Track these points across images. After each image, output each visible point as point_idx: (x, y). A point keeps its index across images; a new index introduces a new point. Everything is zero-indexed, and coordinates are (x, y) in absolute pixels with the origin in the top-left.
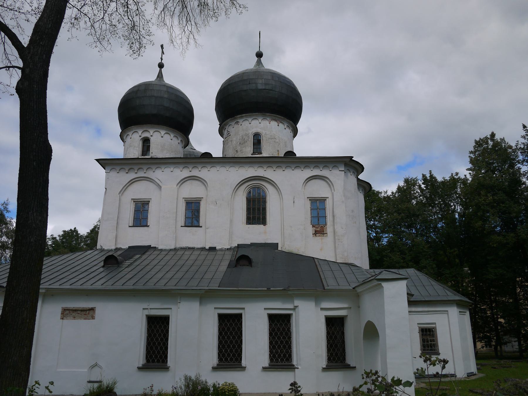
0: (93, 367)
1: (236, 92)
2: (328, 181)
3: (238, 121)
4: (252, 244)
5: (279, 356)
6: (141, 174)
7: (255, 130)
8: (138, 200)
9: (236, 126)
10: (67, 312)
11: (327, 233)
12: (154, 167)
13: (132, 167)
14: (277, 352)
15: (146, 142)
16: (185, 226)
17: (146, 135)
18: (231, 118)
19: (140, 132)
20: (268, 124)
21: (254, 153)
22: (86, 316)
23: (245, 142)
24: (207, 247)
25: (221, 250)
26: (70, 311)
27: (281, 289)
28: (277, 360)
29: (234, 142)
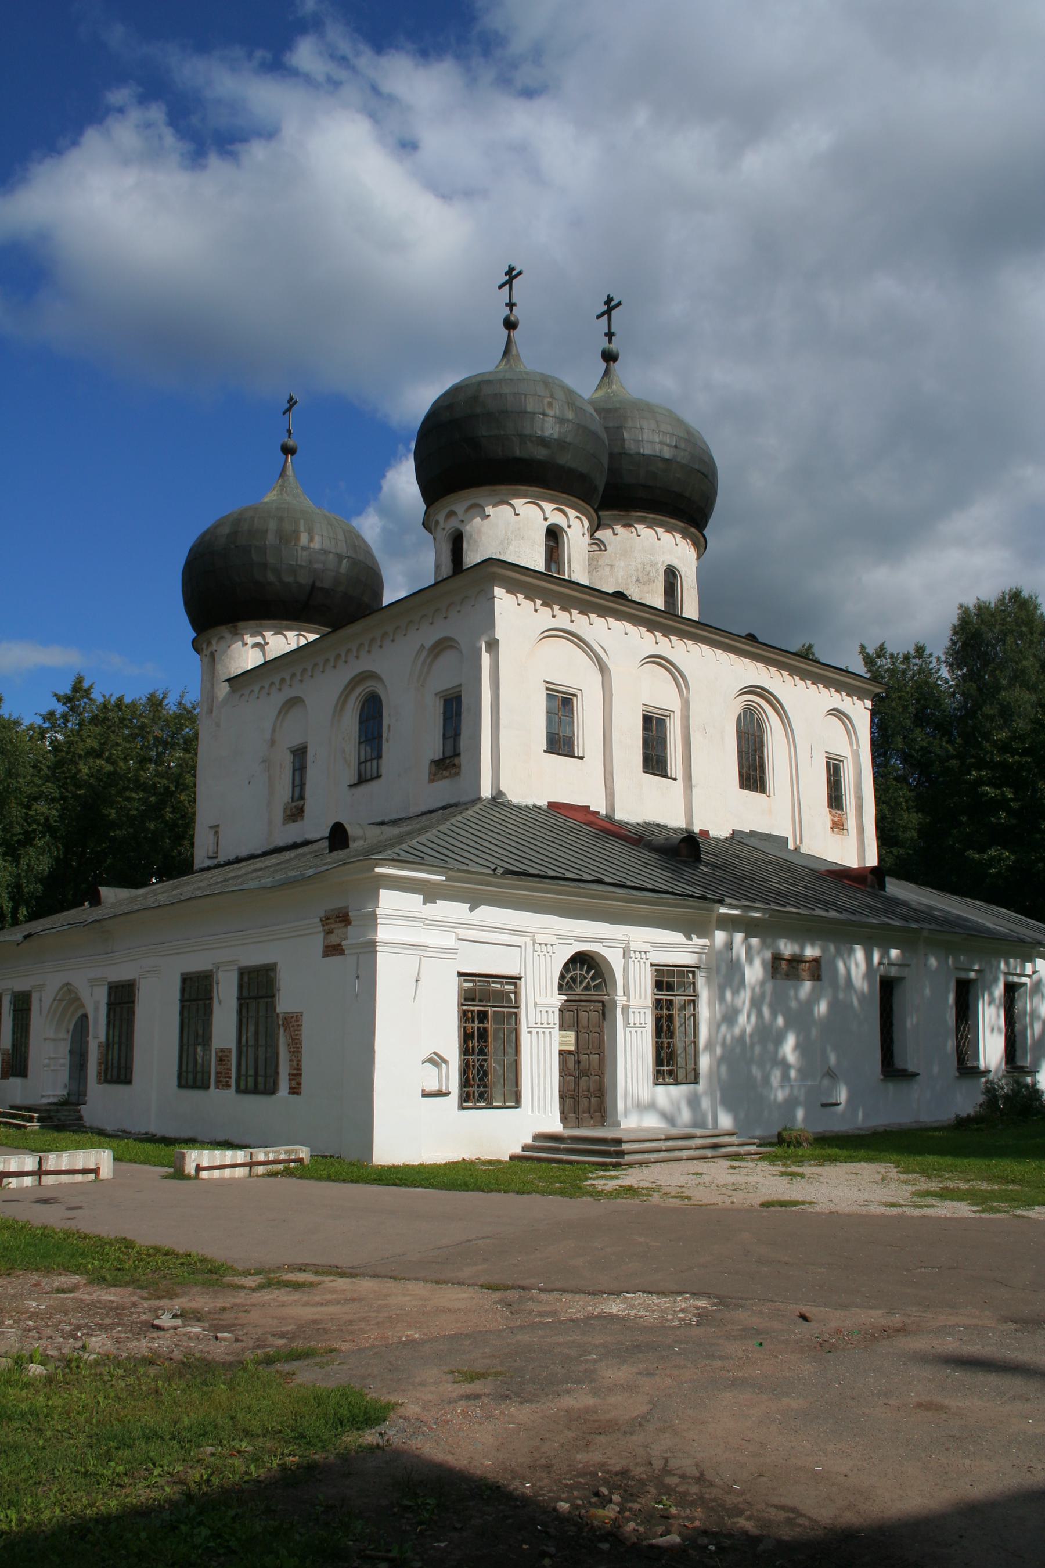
1: (643, 455)
8: (556, 687)
11: (847, 830)
15: (554, 534)
17: (557, 519)
18: (621, 511)
19: (548, 507)
23: (651, 581)
29: (621, 573)
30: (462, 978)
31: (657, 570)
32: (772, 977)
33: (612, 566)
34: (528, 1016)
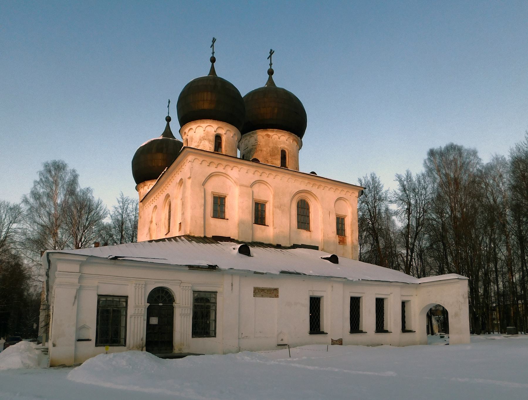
3: (269, 133)
6: (220, 169)
7: (282, 146)
12: (232, 165)
13: (212, 161)
20: (292, 143)
22: (270, 295)
26: (259, 290)
30: (99, 297)
32: (254, 296)
33: (261, 150)
34: (131, 311)
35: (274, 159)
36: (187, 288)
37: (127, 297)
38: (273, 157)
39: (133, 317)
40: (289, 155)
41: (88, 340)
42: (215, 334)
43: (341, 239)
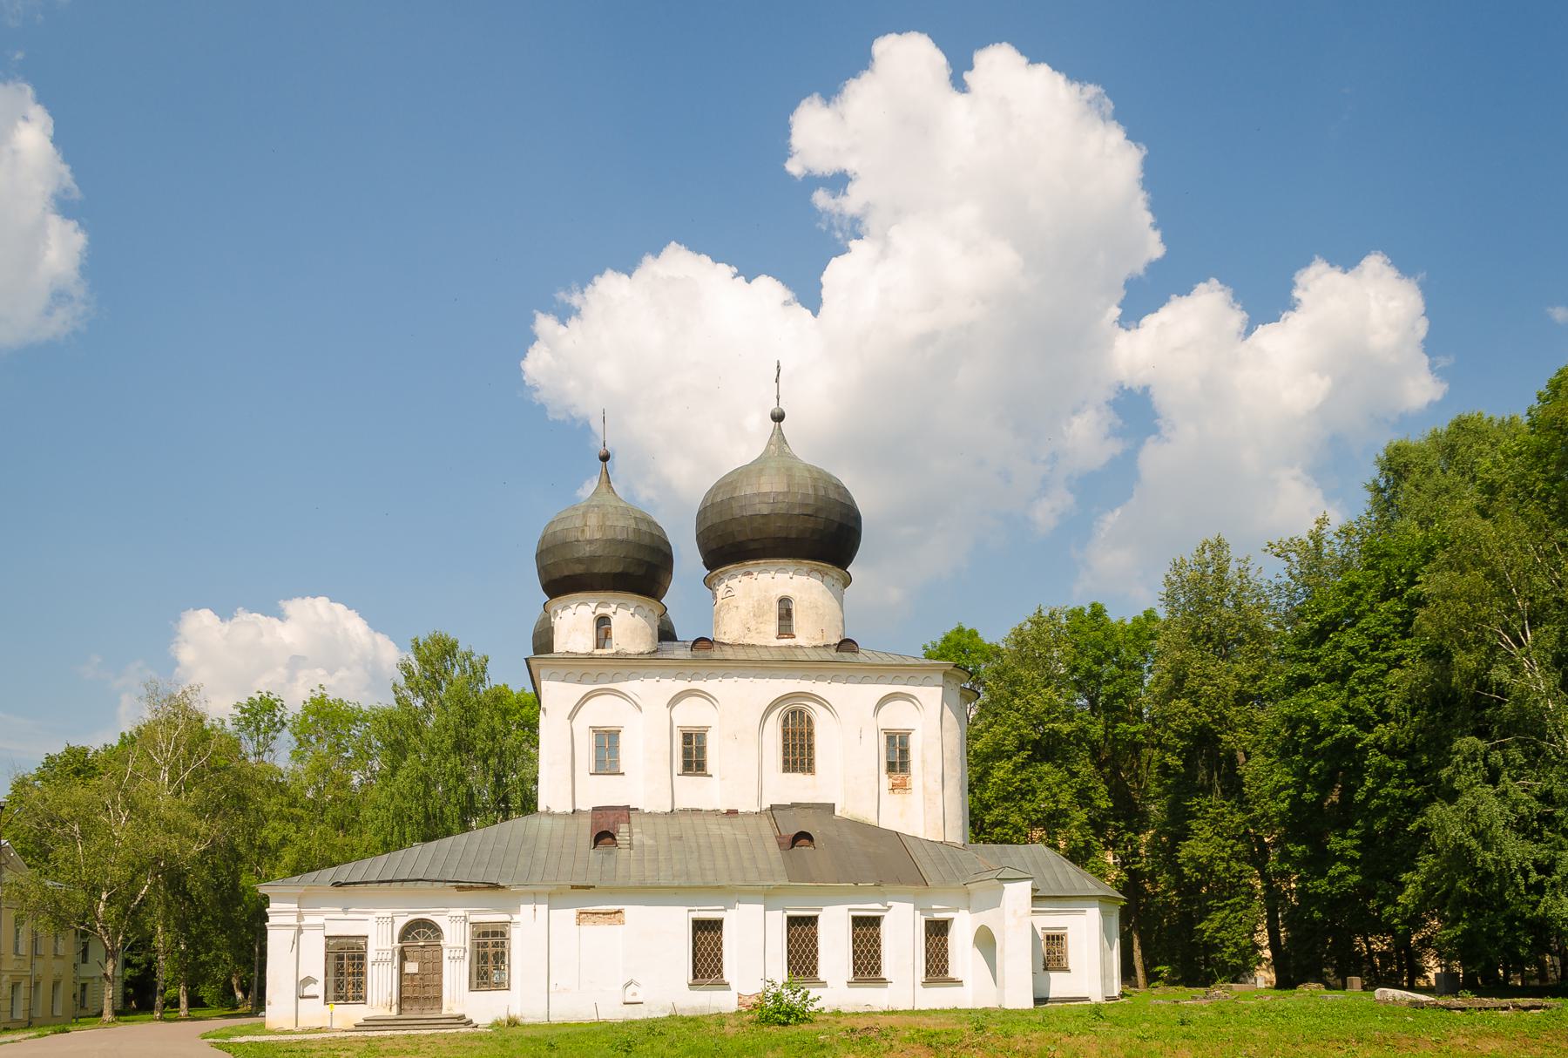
0: (627, 985)
2: (915, 701)
4: (794, 805)
5: (866, 968)
7: (781, 593)
9: (745, 579)
10: (583, 915)
14: (862, 964)
15: (603, 622)
16: (683, 774)
19: (593, 605)
21: (780, 635)
24: (724, 808)
25: (746, 814)
27: (872, 884)
28: (862, 973)
31: (771, 605)
34: (371, 956)
35: (761, 623)
36: (458, 918)
37: (367, 937)
38: (760, 620)
39: (377, 964)
40: (798, 607)
41: (317, 997)
42: (509, 985)
43: (898, 782)
